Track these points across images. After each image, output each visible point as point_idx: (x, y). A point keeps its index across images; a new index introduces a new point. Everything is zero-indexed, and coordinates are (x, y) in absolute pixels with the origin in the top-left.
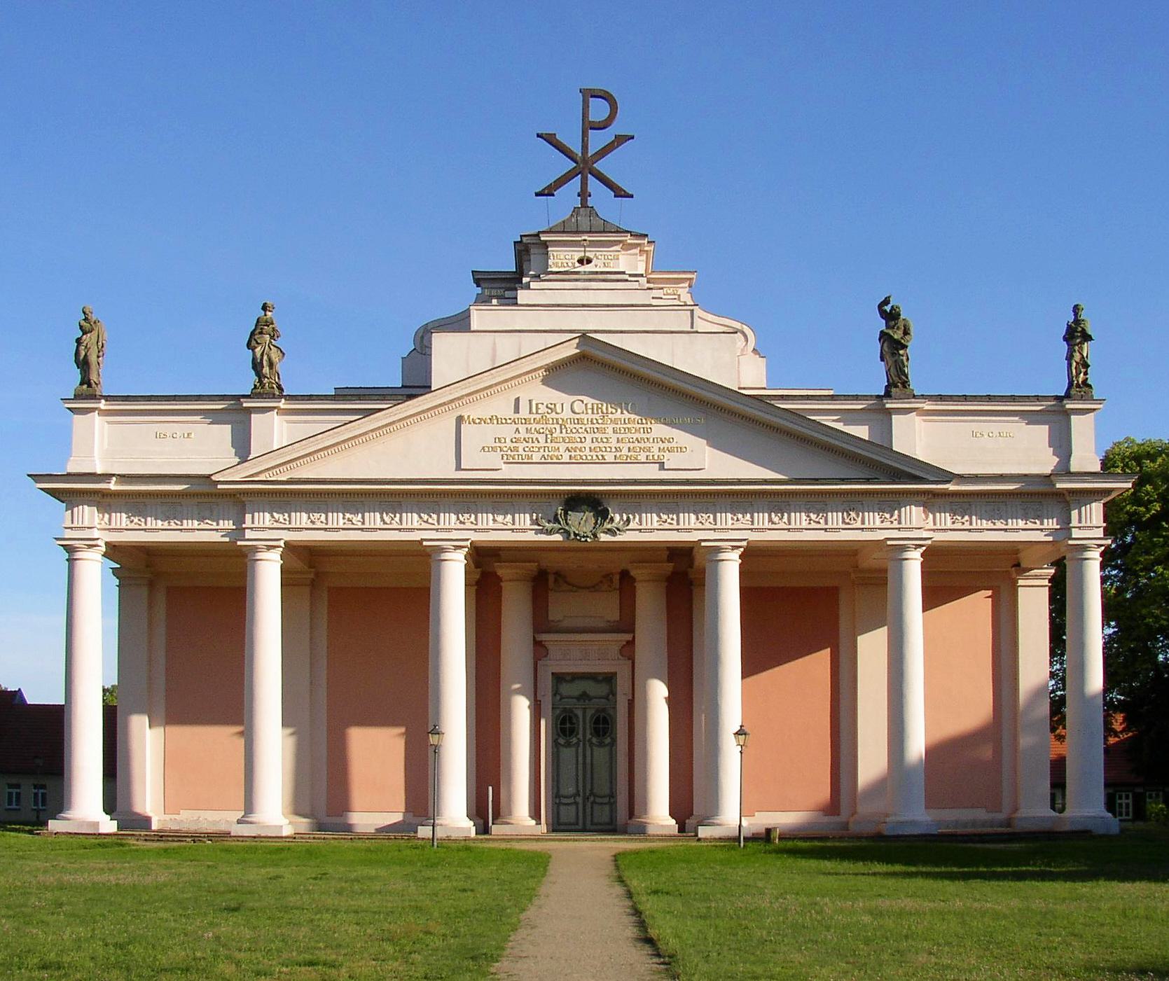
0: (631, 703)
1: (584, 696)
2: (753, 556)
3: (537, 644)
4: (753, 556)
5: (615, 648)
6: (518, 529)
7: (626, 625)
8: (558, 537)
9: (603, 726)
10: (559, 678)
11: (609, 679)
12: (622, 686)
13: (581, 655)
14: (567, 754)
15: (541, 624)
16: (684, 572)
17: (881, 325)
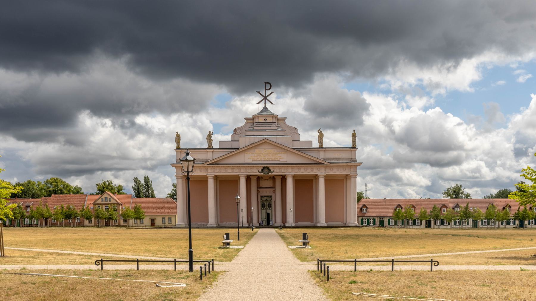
0: (275, 201)
1: (266, 200)
2: (294, 177)
3: (258, 190)
4: (294, 177)
5: (272, 191)
6: (255, 172)
7: (273, 187)
8: (262, 174)
9: (270, 206)
10: (262, 197)
11: (271, 197)
12: (273, 198)
13: (265, 192)
14: (264, 211)
15: (259, 187)
16: (284, 178)
17: (318, 134)
